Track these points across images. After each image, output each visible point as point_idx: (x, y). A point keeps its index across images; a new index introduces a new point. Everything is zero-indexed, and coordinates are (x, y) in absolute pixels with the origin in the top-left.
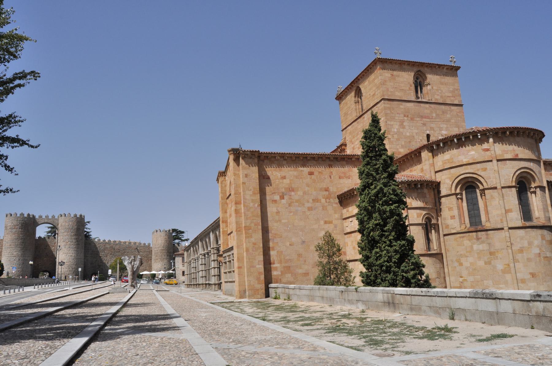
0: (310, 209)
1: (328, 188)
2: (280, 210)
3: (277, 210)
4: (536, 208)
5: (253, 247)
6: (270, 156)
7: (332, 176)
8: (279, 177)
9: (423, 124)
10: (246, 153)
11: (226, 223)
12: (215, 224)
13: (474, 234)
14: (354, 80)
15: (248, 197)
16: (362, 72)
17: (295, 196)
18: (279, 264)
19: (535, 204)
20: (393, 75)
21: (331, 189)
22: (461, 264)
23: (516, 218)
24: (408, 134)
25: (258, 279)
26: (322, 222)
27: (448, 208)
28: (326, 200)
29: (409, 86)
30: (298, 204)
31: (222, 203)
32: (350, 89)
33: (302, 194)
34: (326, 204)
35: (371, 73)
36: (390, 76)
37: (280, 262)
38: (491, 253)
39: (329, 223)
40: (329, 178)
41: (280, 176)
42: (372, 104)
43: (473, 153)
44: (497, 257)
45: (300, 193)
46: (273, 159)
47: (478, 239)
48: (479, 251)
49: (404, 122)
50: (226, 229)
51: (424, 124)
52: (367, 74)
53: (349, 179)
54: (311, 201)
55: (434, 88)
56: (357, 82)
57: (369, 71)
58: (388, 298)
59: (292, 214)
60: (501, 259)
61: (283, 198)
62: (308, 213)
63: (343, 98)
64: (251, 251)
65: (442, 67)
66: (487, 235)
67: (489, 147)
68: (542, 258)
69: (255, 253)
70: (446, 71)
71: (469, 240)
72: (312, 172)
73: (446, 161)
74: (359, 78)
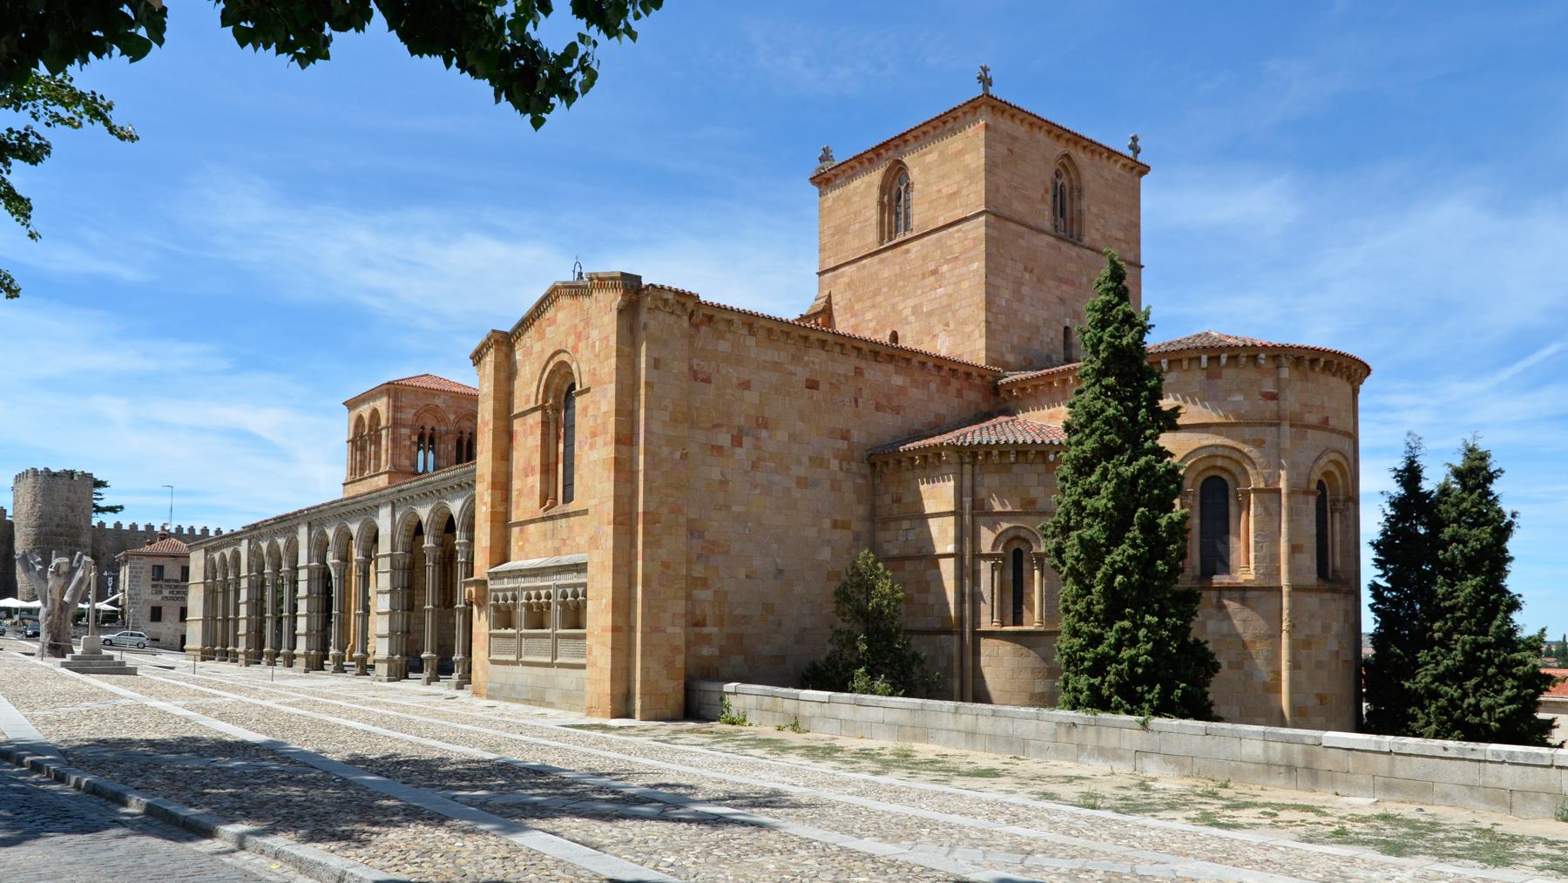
0: (802, 483)
1: (849, 431)
2: (729, 477)
3: (722, 474)
5: (663, 573)
6: (718, 316)
7: (860, 400)
8: (735, 381)
9: (1061, 299)
10: (665, 296)
12: (420, 486)
14: (892, 139)
16: (924, 124)
17: (774, 441)
18: (716, 626)
20: (1011, 151)
21: (856, 436)
24: (1027, 319)
25: (669, 665)
26: (827, 523)
28: (840, 463)
29: (1043, 191)
30: (773, 464)
32: (866, 163)
34: (840, 476)
35: (953, 132)
36: (1005, 152)
37: (720, 622)
39: (843, 528)
40: (853, 405)
43: (1239, 398)
45: (782, 435)
46: (722, 327)
49: (1022, 284)
51: (1062, 301)
52: (938, 132)
54: (805, 460)
55: (1094, 209)
56: (897, 146)
57: (949, 126)
59: (758, 491)
61: (740, 445)
62: (797, 493)
63: (838, 182)
64: (655, 584)
65: (1114, 158)
67: (1275, 391)
69: (665, 592)
70: (1120, 171)
74: (908, 137)
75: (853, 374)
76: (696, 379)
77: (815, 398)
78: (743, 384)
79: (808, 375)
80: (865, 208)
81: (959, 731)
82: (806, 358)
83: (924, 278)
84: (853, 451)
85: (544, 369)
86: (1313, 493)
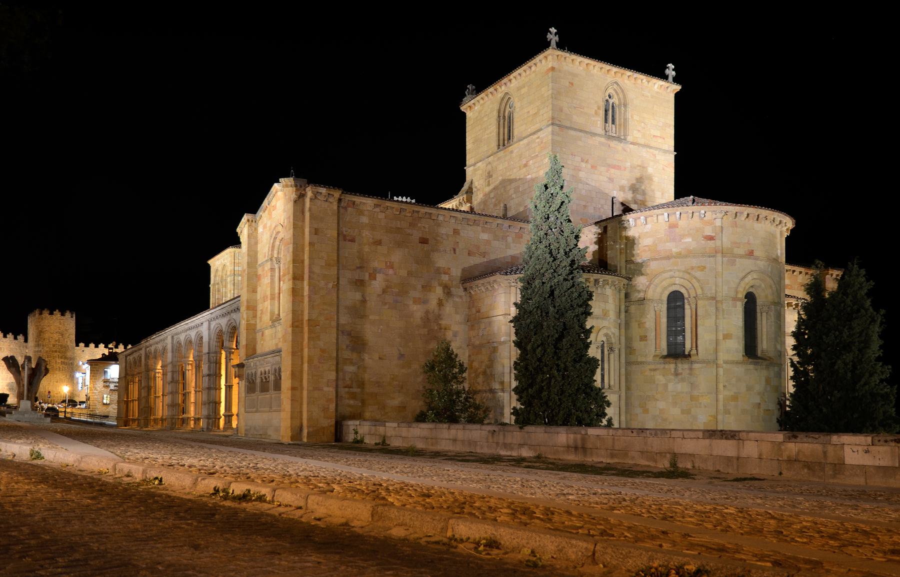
4: (764, 337)
7: (457, 250)
9: (610, 179)
11: (253, 310)
13: (672, 366)
15: (317, 270)
18: (359, 388)
19: (765, 330)
22: (646, 411)
23: (735, 345)
25: (325, 409)
27: (637, 323)
29: (596, 108)
31: (248, 273)
33: (406, 275)
38: (692, 398)
40: (452, 252)
41: (373, 239)
42: (530, 130)
44: (701, 403)
47: (676, 374)
48: (675, 394)
49: (580, 171)
50: (252, 322)
53: (484, 257)
54: (419, 287)
58: (575, 440)
59: (387, 307)
60: (705, 406)
66: (691, 369)
68: (762, 411)
71: (664, 376)
72: (424, 238)
73: (646, 248)
75: (452, 234)
76: (345, 240)
77: (425, 249)
78: (377, 242)
79: (420, 235)
80: (490, 125)
81: (450, 439)
82: (419, 225)
83: (520, 170)
84: (452, 281)
85: (271, 237)
86: (739, 300)
